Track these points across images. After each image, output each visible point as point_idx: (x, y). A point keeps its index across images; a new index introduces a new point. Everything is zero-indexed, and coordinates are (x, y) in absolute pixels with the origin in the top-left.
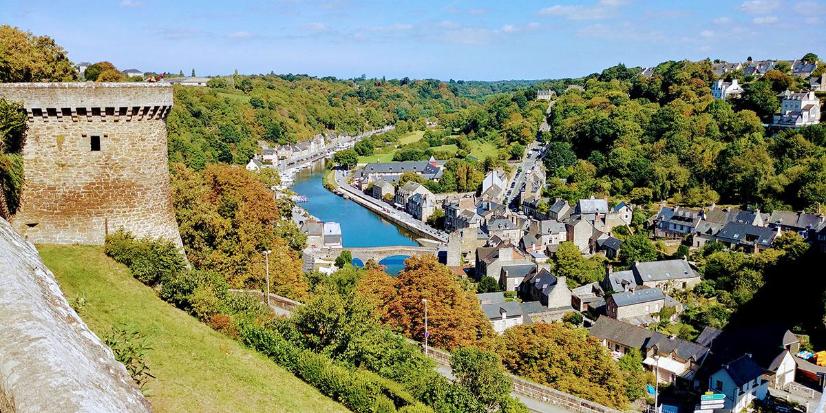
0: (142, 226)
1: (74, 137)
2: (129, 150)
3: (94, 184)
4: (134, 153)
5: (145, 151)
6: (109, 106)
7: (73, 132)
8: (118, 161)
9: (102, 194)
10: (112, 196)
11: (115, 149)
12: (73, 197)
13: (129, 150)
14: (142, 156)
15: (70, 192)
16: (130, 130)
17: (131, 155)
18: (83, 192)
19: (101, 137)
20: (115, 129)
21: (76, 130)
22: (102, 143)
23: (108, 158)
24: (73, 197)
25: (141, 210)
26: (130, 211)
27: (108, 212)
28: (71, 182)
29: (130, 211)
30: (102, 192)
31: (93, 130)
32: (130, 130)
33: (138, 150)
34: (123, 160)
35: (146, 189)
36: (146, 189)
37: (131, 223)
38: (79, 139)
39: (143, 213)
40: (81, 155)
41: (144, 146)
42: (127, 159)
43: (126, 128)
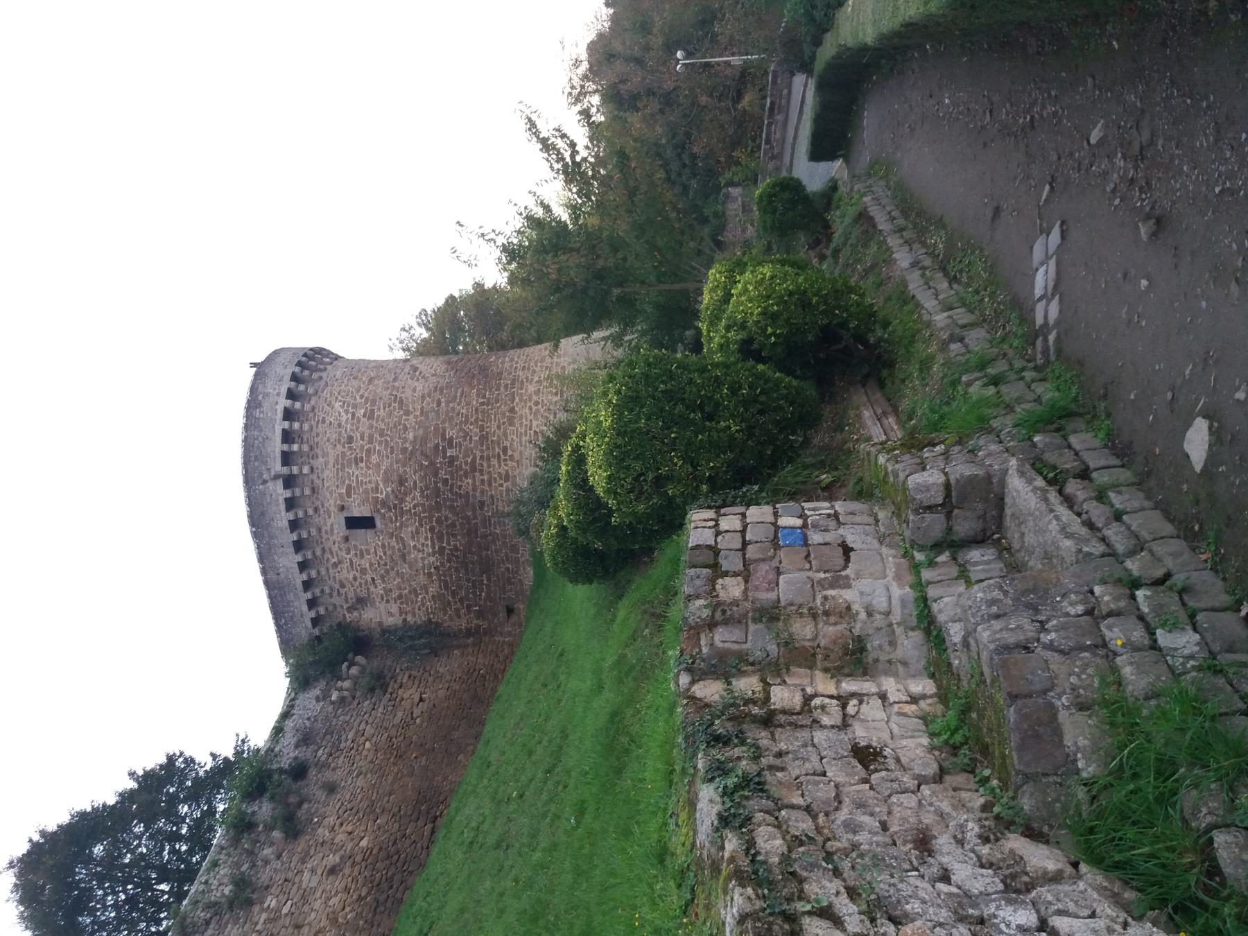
0: (510, 452)
2: (369, 468)
3: (432, 529)
4: (374, 458)
5: (371, 437)
6: (283, 507)
7: (343, 553)
11: (366, 491)
12: (457, 557)
13: (369, 468)
14: (380, 443)
15: (449, 561)
16: (331, 466)
17: (378, 466)
18: (449, 544)
19: (346, 514)
20: (331, 493)
21: (340, 549)
22: (356, 513)
23: (384, 503)
25: (482, 451)
27: (481, 508)
28: (432, 559)
29: (481, 471)
31: (336, 526)
32: (331, 466)
33: (369, 451)
34: (386, 481)
35: (444, 438)
36: (444, 438)
38: (355, 547)
39: (488, 448)
40: (383, 546)
41: (362, 439)
42: (386, 473)
43: (327, 472)
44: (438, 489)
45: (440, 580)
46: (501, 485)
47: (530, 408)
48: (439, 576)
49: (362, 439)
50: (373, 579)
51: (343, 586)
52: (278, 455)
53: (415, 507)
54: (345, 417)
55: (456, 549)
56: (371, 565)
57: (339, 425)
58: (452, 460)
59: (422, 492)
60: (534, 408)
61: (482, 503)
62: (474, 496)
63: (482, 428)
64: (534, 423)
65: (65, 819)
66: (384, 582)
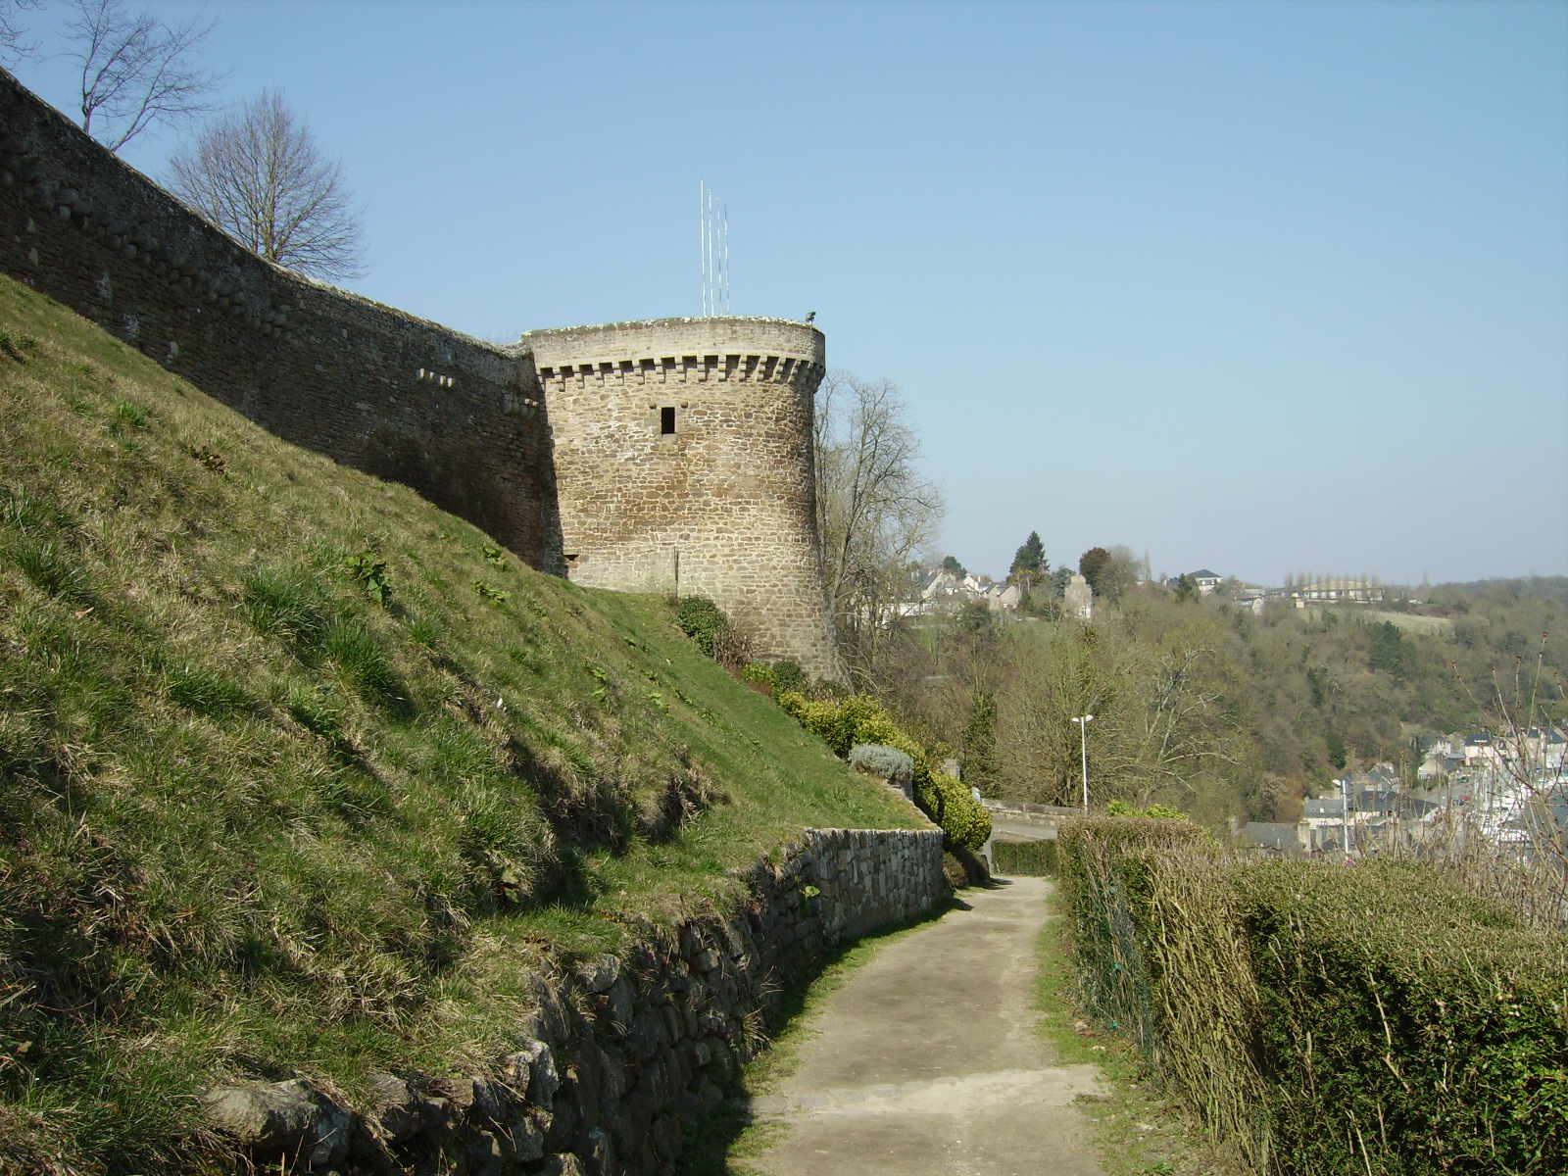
0: (735, 566)
1: (638, 411)
3: (663, 488)
8: (701, 450)
9: (674, 506)
10: (690, 509)
12: (631, 510)
16: (725, 397)
18: (644, 503)
19: (678, 409)
21: (641, 399)
24: (631, 510)
25: (737, 538)
26: (717, 538)
27: (681, 537)
30: (674, 502)
32: (725, 397)
37: (716, 559)
39: (740, 545)
44: (701, 495)
45: (607, 491)
46: (704, 557)
47: (775, 586)
48: (612, 490)
49: (749, 427)
50: (610, 427)
51: (603, 398)
52: (735, 352)
53: (684, 474)
54: (766, 409)
55: (641, 510)
56: (625, 427)
57: (762, 406)
58: (728, 511)
59: (698, 481)
60: (776, 589)
61: (687, 537)
62: (693, 530)
63: (757, 539)
64: (762, 590)
65: (1475, 579)
66: (607, 437)
